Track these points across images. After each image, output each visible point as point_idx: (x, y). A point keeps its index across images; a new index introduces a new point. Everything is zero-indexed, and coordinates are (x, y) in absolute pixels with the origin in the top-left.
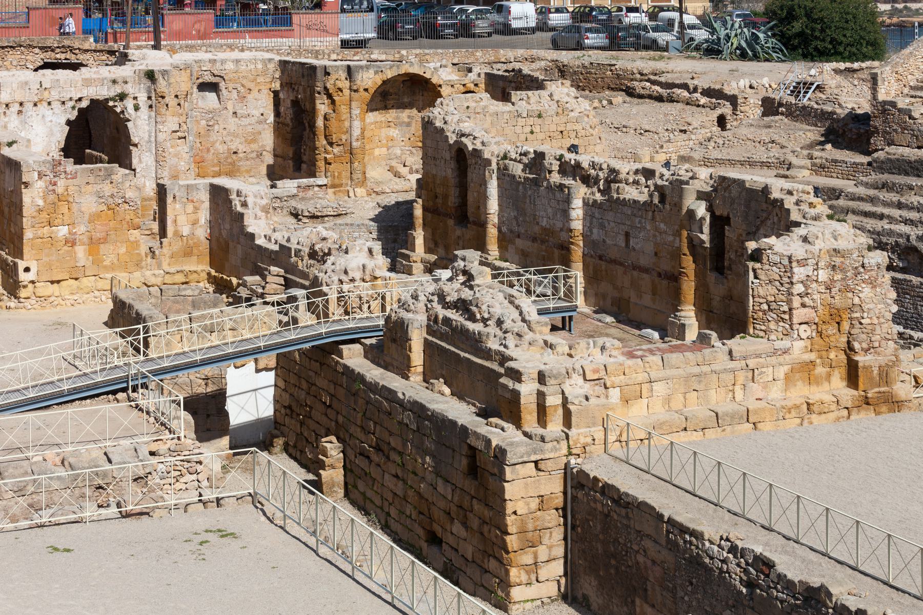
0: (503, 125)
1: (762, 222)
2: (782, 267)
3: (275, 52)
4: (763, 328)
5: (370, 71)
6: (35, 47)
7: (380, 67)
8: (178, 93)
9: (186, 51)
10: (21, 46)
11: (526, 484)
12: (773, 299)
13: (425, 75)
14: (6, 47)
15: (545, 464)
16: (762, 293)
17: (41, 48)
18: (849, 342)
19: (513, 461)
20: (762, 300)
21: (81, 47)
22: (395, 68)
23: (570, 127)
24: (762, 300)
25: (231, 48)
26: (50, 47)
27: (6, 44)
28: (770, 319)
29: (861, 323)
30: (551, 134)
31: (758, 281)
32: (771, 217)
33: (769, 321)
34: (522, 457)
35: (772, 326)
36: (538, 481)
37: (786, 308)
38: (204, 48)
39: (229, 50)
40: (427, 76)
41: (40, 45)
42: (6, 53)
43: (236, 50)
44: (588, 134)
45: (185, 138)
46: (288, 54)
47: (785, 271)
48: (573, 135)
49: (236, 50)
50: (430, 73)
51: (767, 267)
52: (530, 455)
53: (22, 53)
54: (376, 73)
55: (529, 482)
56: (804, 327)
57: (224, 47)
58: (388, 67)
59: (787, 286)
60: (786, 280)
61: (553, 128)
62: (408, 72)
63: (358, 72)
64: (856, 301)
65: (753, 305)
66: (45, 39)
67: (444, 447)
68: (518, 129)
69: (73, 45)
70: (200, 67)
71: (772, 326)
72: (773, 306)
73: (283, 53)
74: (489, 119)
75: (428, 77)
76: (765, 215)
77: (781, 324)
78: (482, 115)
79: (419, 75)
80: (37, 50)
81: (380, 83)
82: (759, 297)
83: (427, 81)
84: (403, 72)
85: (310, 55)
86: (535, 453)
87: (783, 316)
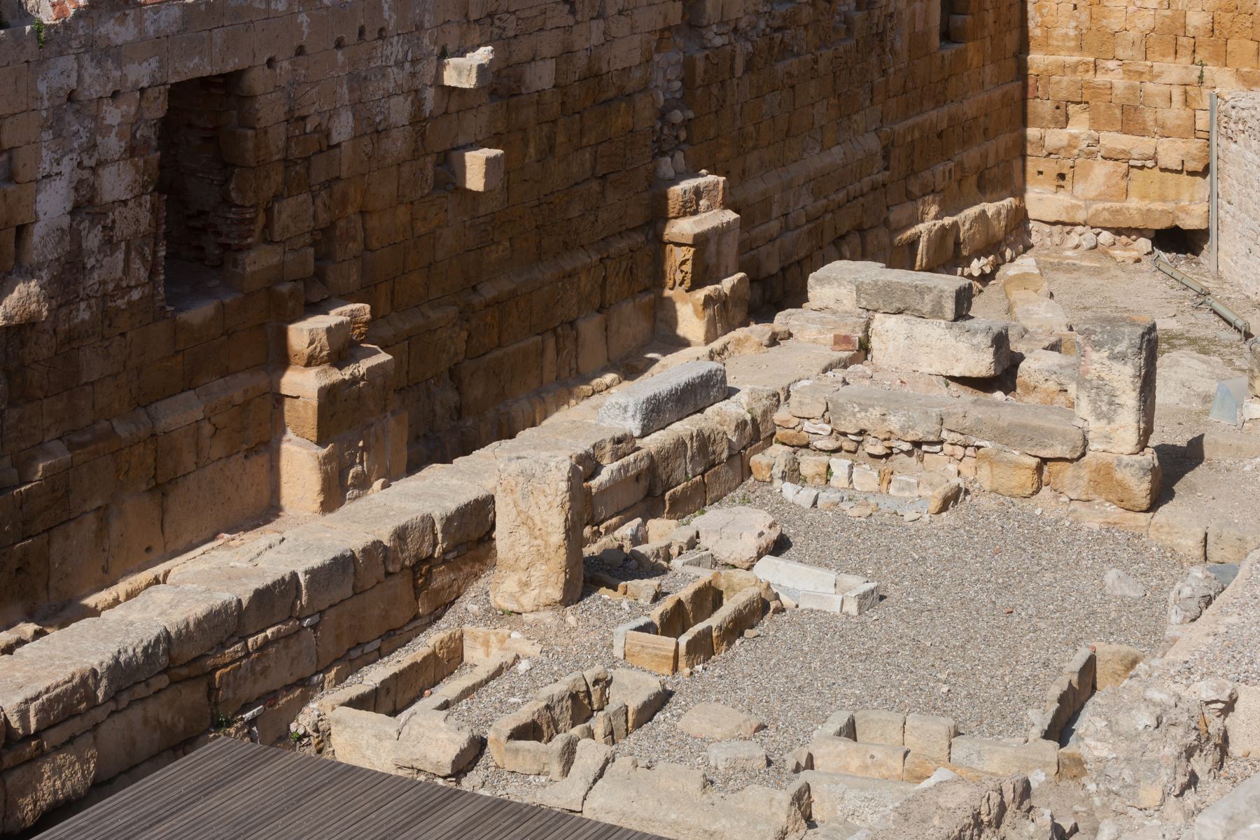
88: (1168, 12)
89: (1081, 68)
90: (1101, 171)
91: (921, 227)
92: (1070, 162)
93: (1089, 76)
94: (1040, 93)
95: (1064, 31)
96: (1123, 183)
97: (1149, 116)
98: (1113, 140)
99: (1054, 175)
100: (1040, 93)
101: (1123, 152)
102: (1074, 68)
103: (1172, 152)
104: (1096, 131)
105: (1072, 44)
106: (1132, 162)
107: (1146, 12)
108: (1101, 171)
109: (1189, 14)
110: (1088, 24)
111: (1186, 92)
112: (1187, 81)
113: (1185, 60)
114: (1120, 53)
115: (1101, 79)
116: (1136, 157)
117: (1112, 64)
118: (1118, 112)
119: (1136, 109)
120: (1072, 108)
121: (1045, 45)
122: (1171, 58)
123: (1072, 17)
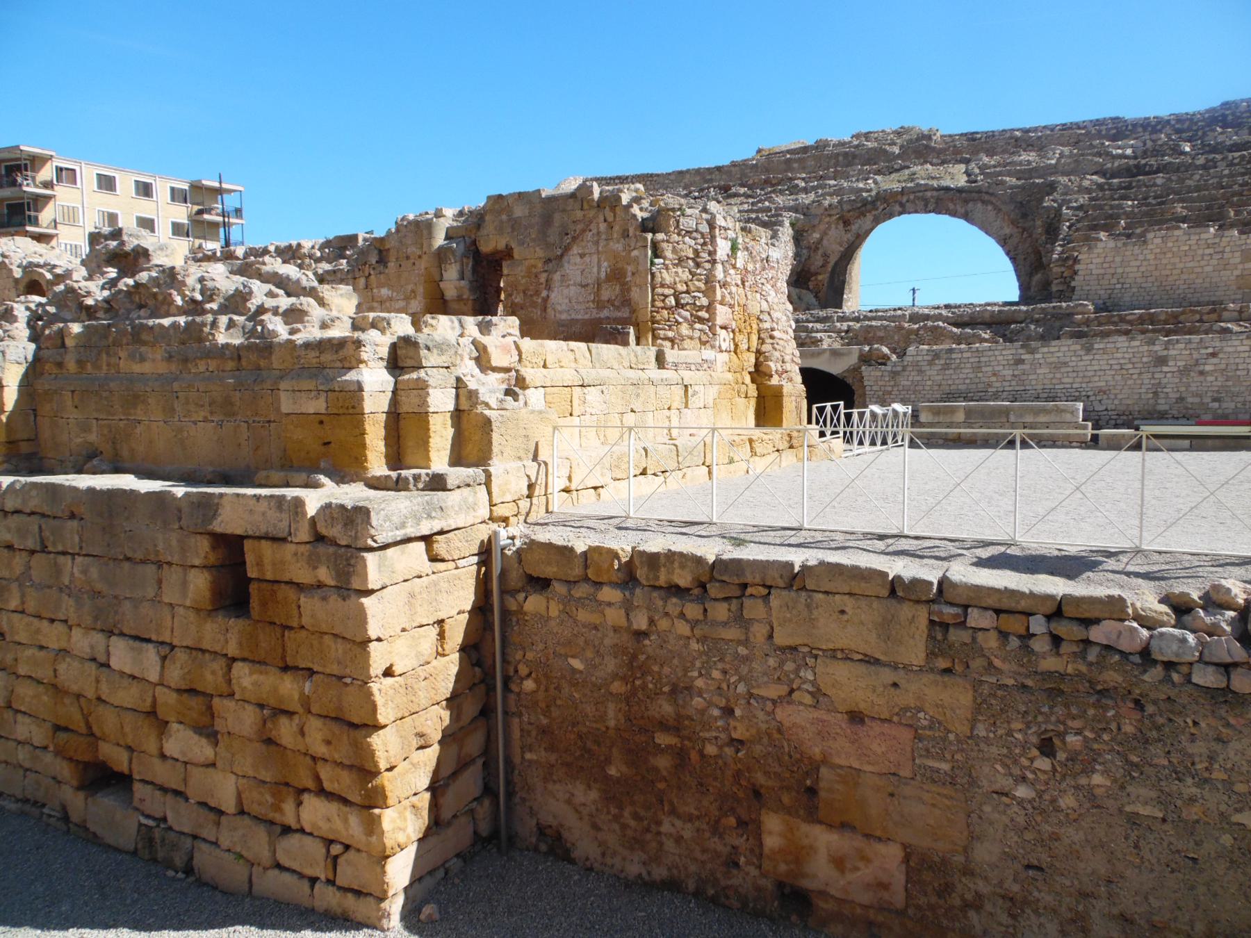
1: (574, 239)
2: (699, 236)
4: (670, 334)
11: (412, 595)
12: (684, 288)
15: (448, 542)
16: (668, 279)
18: (757, 365)
19: (382, 538)
20: (667, 291)
24: (667, 291)
28: (680, 320)
29: (772, 337)
31: (661, 261)
32: (593, 226)
33: (679, 323)
34: (403, 525)
35: (685, 330)
36: (435, 584)
37: (705, 302)
47: (704, 244)
51: (675, 237)
52: (418, 520)
55: (417, 590)
56: (723, 333)
59: (708, 266)
60: (705, 256)
64: (765, 306)
65: (653, 300)
67: (126, 565)
71: (685, 330)
72: (686, 299)
76: (579, 227)
77: (697, 326)
82: (662, 286)
86: (429, 517)
87: (700, 314)
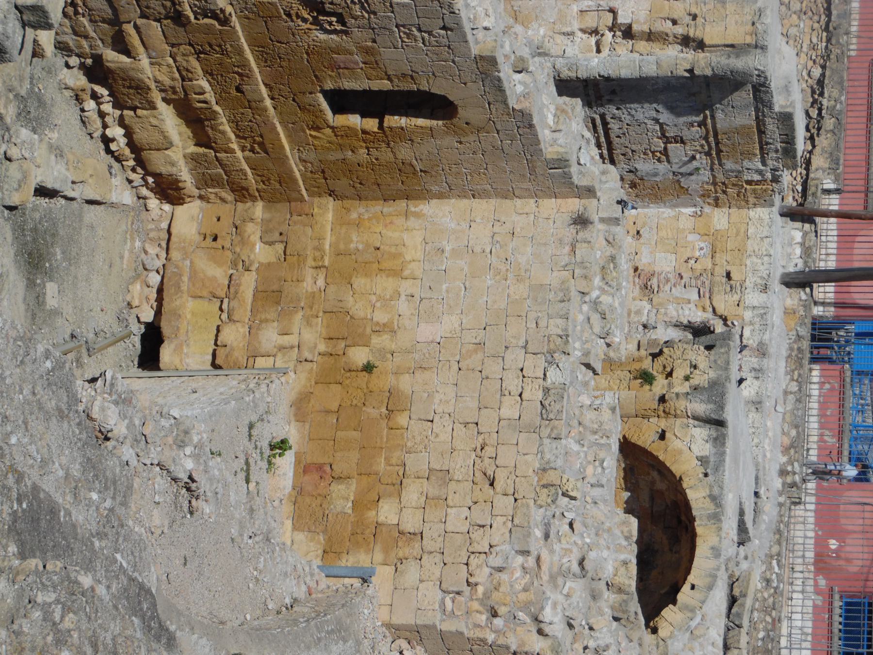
0: (532, 316)
3: (775, 549)
5: (708, 446)
6: (823, 67)
7: (717, 469)
8: (700, 20)
9: (791, 349)
10: (829, 40)
13: (686, 588)
14: (829, 14)
17: (821, 82)
21: (818, 150)
22: (711, 507)
23: (504, 504)
25: (792, 446)
26: (822, 94)
27: (834, 12)
30: (489, 451)
38: (794, 387)
39: (787, 441)
40: (685, 595)
41: (828, 73)
42: (816, 18)
43: (784, 459)
44: (474, 561)
45: (599, 51)
46: (768, 581)
48: (480, 515)
49: (784, 459)
50: (692, 602)
53: (814, 48)
54: (703, 460)
57: (794, 433)
58: (716, 491)
61: (507, 456)
62: (699, 541)
63: (709, 401)
66: (841, 83)
68: (515, 357)
69: (822, 137)
70: (751, 323)
73: (770, 568)
74: (554, 278)
75: (680, 597)
78: (566, 259)
79: (688, 571)
80: (817, 72)
81: (677, 469)
83: (671, 597)
84: (699, 530)
85: (761, 635)
88: (368, 330)
89: (317, 254)
90: (218, 273)
91: (145, 61)
92: (227, 245)
93: (310, 262)
94: (295, 218)
95: (354, 238)
96: (205, 293)
97: (271, 314)
98: (248, 283)
99: (216, 232)
100: (295, 218)
101: (236, 293)
102: (319, 248)
103: (232, 335)
104: (257, 269)
105: (342, 246)
106: (226, 301)
107: (369, 311)
108: (218, 273)
109: (367, 349)
110: (360, 259)
111: (292, 347)
112: (302, 348)
113: (322, 347)
114: (332, 289)
115: (309, 273)
116: (231, 304)
117: (321, 282)
118: (275, 287)
119: (278, 303)
120: (280, 247)
121: (341, 221)
122: (324, 335)
123: (367, 245)
